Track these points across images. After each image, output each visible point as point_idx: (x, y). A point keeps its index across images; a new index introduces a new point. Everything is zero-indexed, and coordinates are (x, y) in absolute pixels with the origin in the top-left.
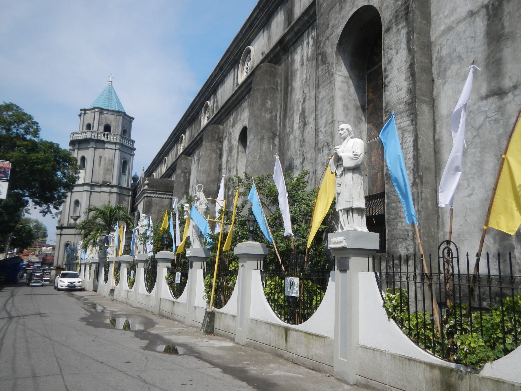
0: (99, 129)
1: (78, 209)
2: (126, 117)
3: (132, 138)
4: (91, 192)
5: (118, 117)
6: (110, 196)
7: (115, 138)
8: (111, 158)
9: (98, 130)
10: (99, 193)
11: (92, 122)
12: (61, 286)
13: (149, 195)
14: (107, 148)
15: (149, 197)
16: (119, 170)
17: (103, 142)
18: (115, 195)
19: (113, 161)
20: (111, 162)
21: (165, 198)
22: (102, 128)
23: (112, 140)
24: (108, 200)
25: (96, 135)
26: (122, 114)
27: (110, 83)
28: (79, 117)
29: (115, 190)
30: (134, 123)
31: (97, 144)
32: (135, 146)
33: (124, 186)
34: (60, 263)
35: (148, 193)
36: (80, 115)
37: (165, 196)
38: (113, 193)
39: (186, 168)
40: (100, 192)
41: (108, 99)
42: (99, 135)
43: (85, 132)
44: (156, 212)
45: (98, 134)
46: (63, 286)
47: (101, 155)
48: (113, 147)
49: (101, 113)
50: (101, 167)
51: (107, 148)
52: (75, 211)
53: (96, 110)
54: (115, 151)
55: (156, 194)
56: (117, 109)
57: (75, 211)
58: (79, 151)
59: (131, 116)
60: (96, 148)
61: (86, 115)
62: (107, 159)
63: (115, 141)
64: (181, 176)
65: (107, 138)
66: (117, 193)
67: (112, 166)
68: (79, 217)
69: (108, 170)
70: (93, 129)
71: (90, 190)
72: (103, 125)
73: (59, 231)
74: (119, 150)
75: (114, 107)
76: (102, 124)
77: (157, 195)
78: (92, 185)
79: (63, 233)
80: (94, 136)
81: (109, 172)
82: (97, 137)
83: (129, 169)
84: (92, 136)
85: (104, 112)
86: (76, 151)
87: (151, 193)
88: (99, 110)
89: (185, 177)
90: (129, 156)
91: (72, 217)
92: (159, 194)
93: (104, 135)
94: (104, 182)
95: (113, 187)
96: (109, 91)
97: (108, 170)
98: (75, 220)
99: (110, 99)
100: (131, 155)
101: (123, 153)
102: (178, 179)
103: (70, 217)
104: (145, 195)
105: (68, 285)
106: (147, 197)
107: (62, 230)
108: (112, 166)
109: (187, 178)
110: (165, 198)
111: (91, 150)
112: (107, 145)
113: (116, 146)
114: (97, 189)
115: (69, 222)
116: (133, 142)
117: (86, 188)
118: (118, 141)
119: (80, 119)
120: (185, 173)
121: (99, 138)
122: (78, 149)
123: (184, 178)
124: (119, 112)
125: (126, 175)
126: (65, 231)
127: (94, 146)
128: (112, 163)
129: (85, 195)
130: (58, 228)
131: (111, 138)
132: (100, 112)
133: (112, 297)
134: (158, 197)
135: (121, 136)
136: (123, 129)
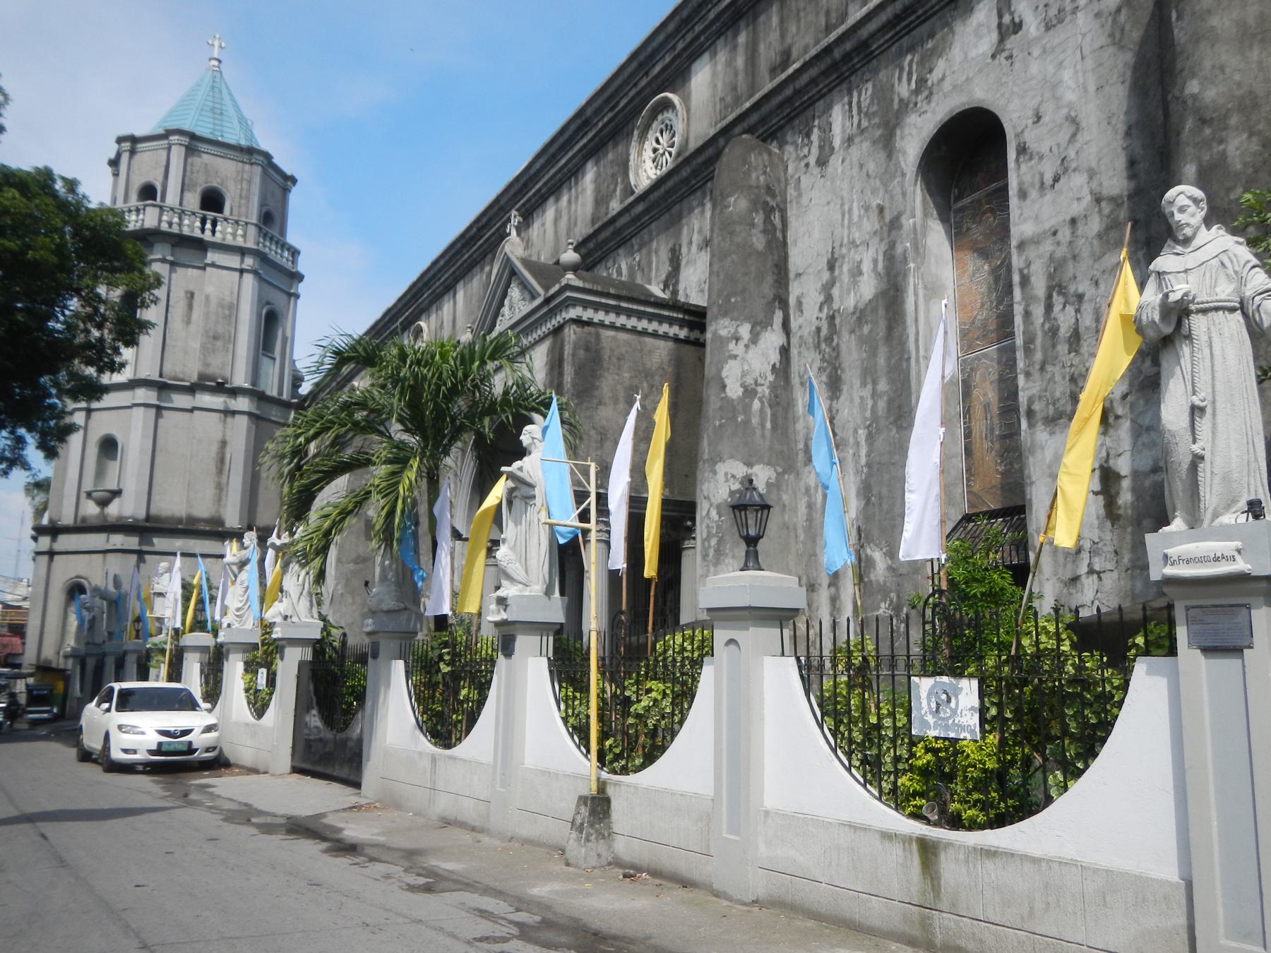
0: (185, 202)
1: (113, 467)
2: (271, 172)
3: (292, 238)
4: (159, 409)
5: (247, 167)
6: (225, 421)
7: (240, 232)
8: (228, 299)
9: (181, 204)
10: (187, 415)
11: (160, 178)
12: (126, 751)
13: (587, 314)
14: (213, 265)
15: (589, 323)
16: (253, 341)
17: (200, 246)
18: (243, 421)
19: (232, 309)
20: (227, 312)
21: (655, 335)
22: (193, 201)
23: (229, 240)
24: (219, 436)
25: (176, 220)
27: (216, 63)
28: (109, 170)
29: (243, 403)
30: (295, 197)
31: (178, 250)
32: (302, 267)
33: (274, 393)
34: (49, 653)
35: (586, 305)
36: (114, 163)
37: (653, 326)
38: (234, 413)
39: (769, 190)
40: (192, 410)
41: (213, 110)
42: (186, 222)
43: (138, 210)
44: (622, 395)
45: (180, 219)
46: (135, 752)
47: (191, 288)
48: (234, 261)
49: (190, 151)
50: (193, 327)
51: (213, 265)
52: (100, 473)
53: (174, 138)
55: (618, 311)
56: (243, 143)
57: (100, 473)
59: (288, 172)
60: (173, 264)
61: (137, 157)
62: (214, 301)
63: (240, 242)
64: (753, 225)
65: (213, 232)
66: (250, 414)
67: (229, 324)
68: (117, 493)
70: (163, 198)
71: (157, 403)
72: (199, 189)
74: (255, 272)
75: (233, 135)
76: (195, 185)
77: (622, 320)
78: (162, 387)
80: (170, 224)
81: (219, 344)
82: (180, 225)
84: (160, 221)
85: (203, 147)
87: (597, 307)
88: (186, 140)
89: (769, 229)
90: (285, 297)
91: (89, 495)
92: (629, 313)
93: (203, 222)
94: (202, 377)
95: (234, 392)
96: (213, 88)
97: (218, 339)
98: (103, 503)
99: (219, 111)
100: (290, 295)
101: (267, 288)
102: (738, 239)
103: (83, 495)
104: (574, 313)
105: (160, 744)
106: (578, 322)
107: (54, 539)
108: (229, 324)
109: (779, 235)
110: (655, 335)
112: (211, 257)
113: (242, 261)
114: (181, 400)
115: (82, 513)
116: (295, 253)
117: (142, 395)
118: (250, 244)
119: (116, 175)
120: (769, 211)
121: (186, 231)
123: (765, 231)
125: (274, 359)
126: (65, 542)
127: (170, 258)
128: (230, 316)
131: (225, 233)
132: (187, 147)
133: (601, 846)
134: (623, 329)
135: (260, 229)
136: (265, 209)
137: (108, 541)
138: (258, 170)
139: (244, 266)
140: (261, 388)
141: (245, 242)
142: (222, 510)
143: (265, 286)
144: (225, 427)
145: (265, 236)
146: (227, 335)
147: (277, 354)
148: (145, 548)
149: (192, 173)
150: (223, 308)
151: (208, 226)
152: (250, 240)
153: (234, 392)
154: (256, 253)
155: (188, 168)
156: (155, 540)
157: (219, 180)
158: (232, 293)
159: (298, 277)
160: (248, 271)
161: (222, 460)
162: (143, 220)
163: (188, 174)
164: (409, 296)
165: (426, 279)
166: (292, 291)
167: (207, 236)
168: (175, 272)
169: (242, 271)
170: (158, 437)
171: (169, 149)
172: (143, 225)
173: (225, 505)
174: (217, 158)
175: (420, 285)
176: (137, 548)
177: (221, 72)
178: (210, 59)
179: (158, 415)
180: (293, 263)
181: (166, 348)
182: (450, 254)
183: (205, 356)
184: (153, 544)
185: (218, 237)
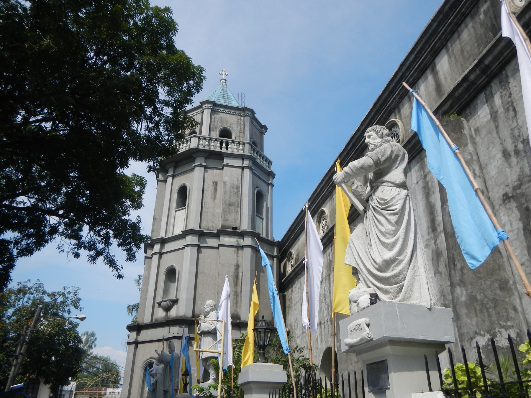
1: (173, 287)
4: (199, 247)
5: (242, 118)
6: (238, 252)
8: (236, 183)
9: (209, 135)
10: (215, 251)
14: (227, 165)
17: (219, 156)
18: (248, 252)
19: (239, 188)
20: (236, 190)
22: (215, 134)
23: (235, 152)
24: (235, 262)
25: (207, 143)
26: (249, 113)
27: (224, 81)
29: (247, 241)
31: (208, 160)
32: (274, 168)
38: (242, 247)
45: (209, 142)
47: (216, 180)
48: (238, 163)
49: (213, 112)
50: (217, 201)
51: (227, 165)
52: (166, 291)
57: (166, 291)
58: (175, 179)
60: (206, 168)
62: (228, 185)
63: (241, 152)
65: (227, 149)
68: (175, 302)
69: (230, 205)
70: (200, 133)
71: (199, 243)
72: (218, 130)
73: (134, 335)
74: (250, 168)
76: (216, 128)
78: (201, 234)
79: (141, 338)
81: (232, 208)
82: (209, 145)
83: (267, 209)
85: (220, 109)
86: (170, 180)
90: (266, 185)
91: (159, 304)
93: (221, 144)
94: (223, 226)
95: (242, 234)
98: (167, 309)
100: (268, 184)
107: (138, 334)
111: (198, 172)
113: (243, 163)
114: (212, 242)
117: (190, 239)
118: (247, 153)
121: (212, 148)
122: (174, 176)
124: (245, 109)
125: (263, 219)
126: (146, 334)
129: (189, 253)
130: (130, 328)
131: (233, 149)
132: (212, 110)
136: (252, 140)
137: (169, 332)
138: (248, 119)
139: (244, 165)
140: (257, 231)
141: (244, 152)
142: (238, 310)
143: (256, 178)
144: (238, 256)
145: (254, 150)
146: (236, 203)
147: (264, 216)
149: (215, 122)
150: (234, 189)
151: (224, 145)
152: (247, 151)
153: (242, 234)
154: (250, 158)
155: (213, 120)
157: (228, 125)
158: (238, 180)
159: (271, 175)
160: (246, 167)
161: (237, 277)
162: (190, 145)
163: (212, 123)
164: (373, 114)
165: (391, 87)
166: (269, 182)
167: (224, 150)
168: (207, 172)
169: (243, 168)
170: (199, 265)
171: (203, 112)
172: (190, 147)
173: (240, 306)
174: (227, 115)
175: (386, 95)
177: (226, 85)
178: (221, 80)
179: (199, 252)
180: (269, 167)
181: (203, 213)
182: (422, 43)
183: (224, 215)
185: (229, 151)
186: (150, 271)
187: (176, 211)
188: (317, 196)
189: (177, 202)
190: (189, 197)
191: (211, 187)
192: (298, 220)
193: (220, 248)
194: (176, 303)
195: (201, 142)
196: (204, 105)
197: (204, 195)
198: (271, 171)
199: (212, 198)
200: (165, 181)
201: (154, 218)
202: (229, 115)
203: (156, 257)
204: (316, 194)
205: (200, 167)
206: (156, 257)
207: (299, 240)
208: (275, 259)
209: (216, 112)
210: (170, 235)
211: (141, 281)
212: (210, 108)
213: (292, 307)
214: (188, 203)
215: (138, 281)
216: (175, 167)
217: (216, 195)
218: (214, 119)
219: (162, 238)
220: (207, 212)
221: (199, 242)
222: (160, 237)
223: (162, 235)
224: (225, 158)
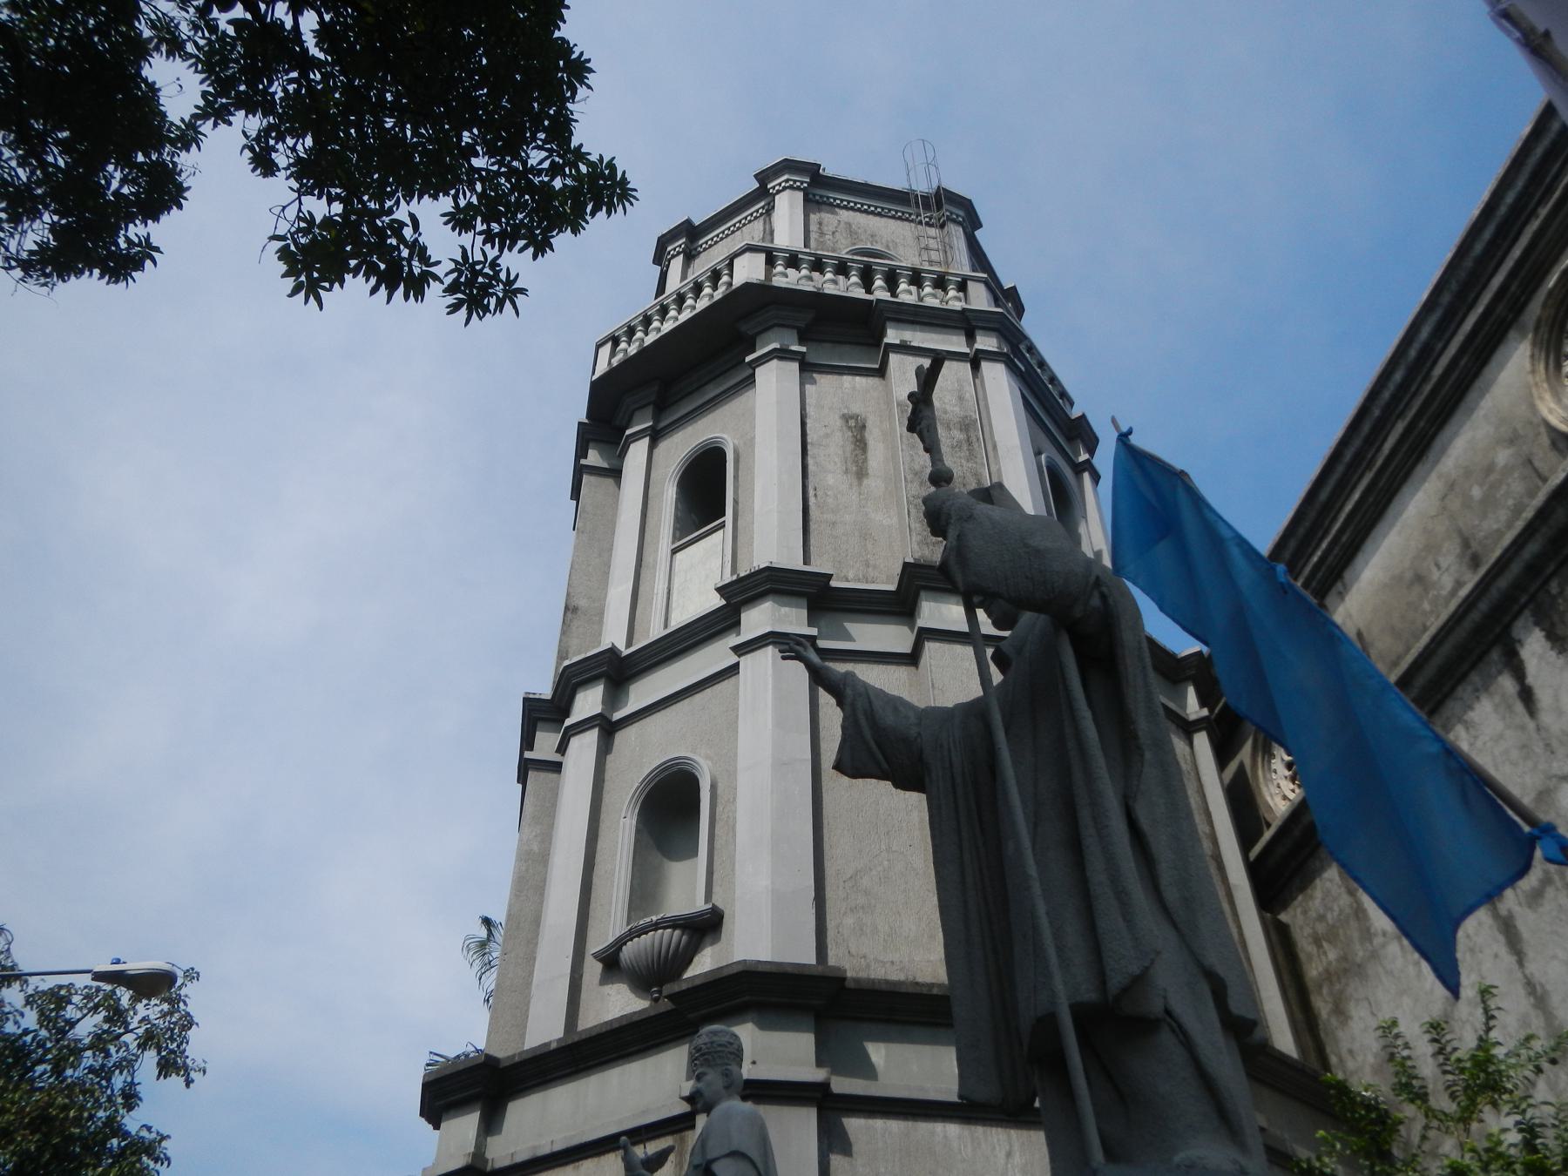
23: (931, 302)
26: (961, 213)
47: (856, 408)
49: (812, 203)
50: (874, 483)
54: (976, 367)
56: (922, 186)
58: (664, 446)
60: (808, 368)
71: (814, 631)
73: (465, 1126)
86: (637, 453)
91: (611, 962)
107: (491, 1124)
108: (971, 456)
122: (656, 436)
132: (807, 200)
138: (957, 234)
139: (977, 346)
148: (843, 1085)
149: (822, 234)
151: (879, 283)
155: (813, 227)
156: (878, 1053)
158: (961, 398)
162: (730, 284)
168: (814, 382)
171: (769, 210)
174: (871, 216)
176: (811, 1073)
181: (813, 526)
184: (867, 1070)
186: (551, 826)
187: (674, 551)
188: (1493, 244)
189: (677, 519)
190: (736, 477)
191: (839, 434)
192: (1324, 495)
193: (931, 648)
194: (708, 939)
195: (779, 269)
196: (770, 182)
197: (810, 461)
198: (1083, 418)
199: (846, 472)
200: (615, 473)
201: (567, 608)
202: (878, 219)
203: (584, 747)
204: (1487, 234)
205: (781, 358)
206: (584, 747)
207: (1342, 596)
208: (1202, 741)
209: (824, 207)
210: (654, 631)
211: (496, 952)
212: (798, 188)
213: (1374, 956)
214: (736, 502)
215: (483, 945)
216: (660, 408)
217: (865, 460)
218: (820, 224)
219: (613, 651)
220: (834, 523)
221: (809, 625)
222: (605, 646)
223: (614, 635)
224: (888, 324)
